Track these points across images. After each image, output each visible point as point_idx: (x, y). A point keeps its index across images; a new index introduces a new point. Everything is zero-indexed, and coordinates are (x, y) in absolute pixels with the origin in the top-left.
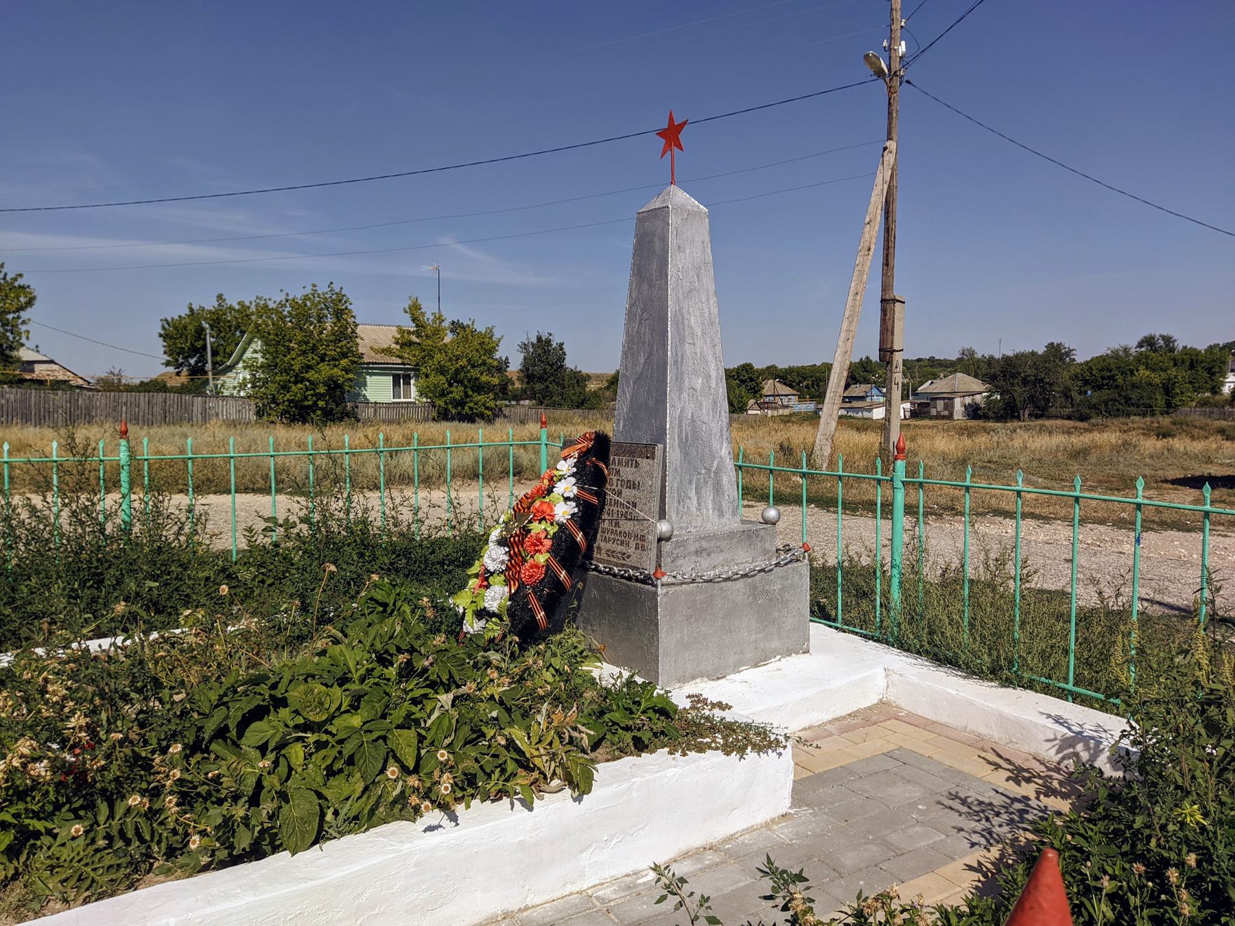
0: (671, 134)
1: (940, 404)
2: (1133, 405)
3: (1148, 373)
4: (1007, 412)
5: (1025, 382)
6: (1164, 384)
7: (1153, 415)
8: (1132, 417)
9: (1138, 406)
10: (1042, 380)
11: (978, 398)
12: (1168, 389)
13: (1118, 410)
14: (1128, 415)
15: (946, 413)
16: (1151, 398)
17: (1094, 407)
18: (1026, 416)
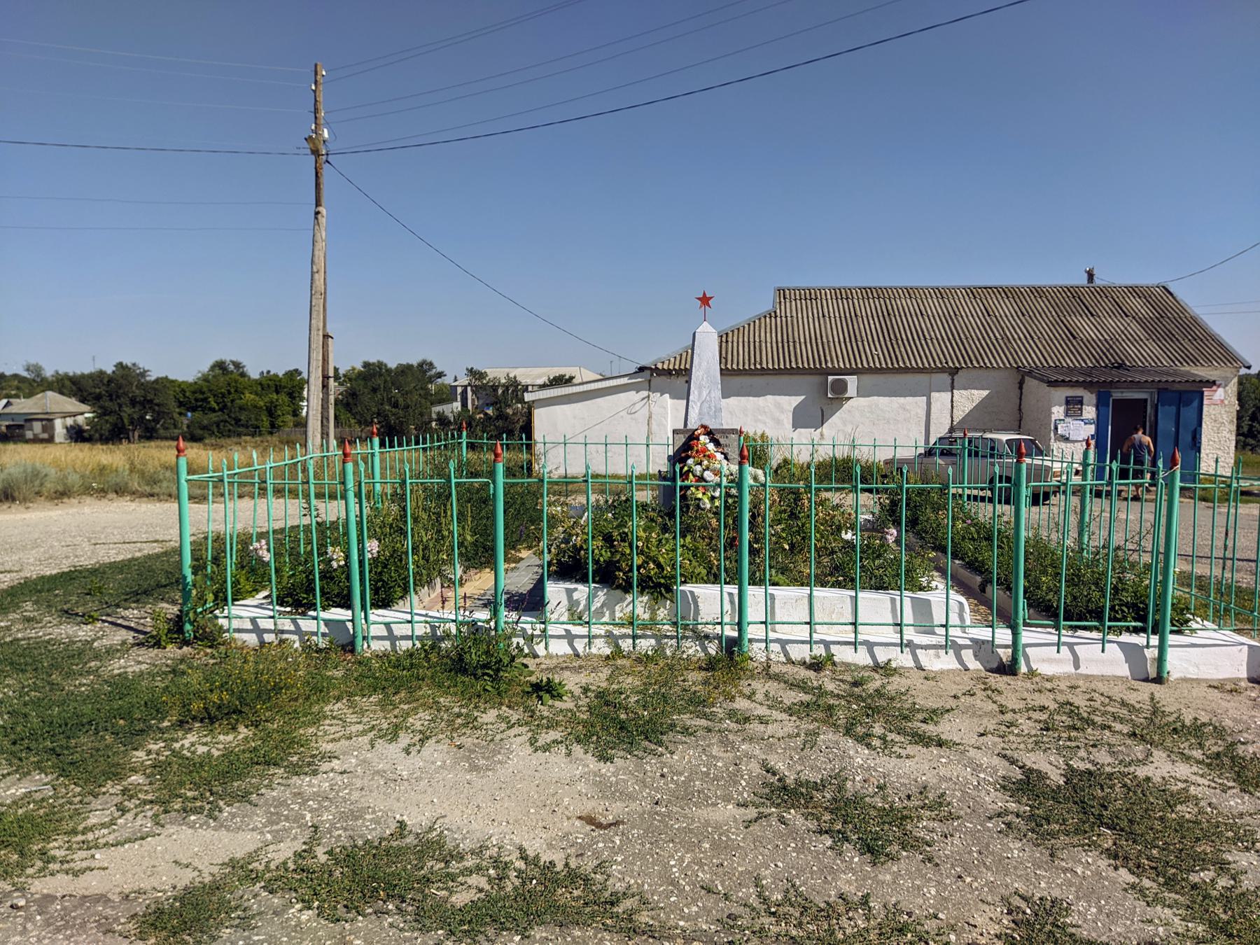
0: (705, 300)
1: (37, 427)
2: (243, 425)
3: (252, 396)
4: (114, 434)
5: (133, 402)
6: (267, 407)
7: (260, 435)
8: (243, 438)
9: (247, 427)
10: (151, 401)
11: (80, 419)
12: (271, 411)
13: (229, 431)
14: (239, 435)
15: (45, 436)
16: (257, 420)
17: (204, 428)
18: (136, 437)
